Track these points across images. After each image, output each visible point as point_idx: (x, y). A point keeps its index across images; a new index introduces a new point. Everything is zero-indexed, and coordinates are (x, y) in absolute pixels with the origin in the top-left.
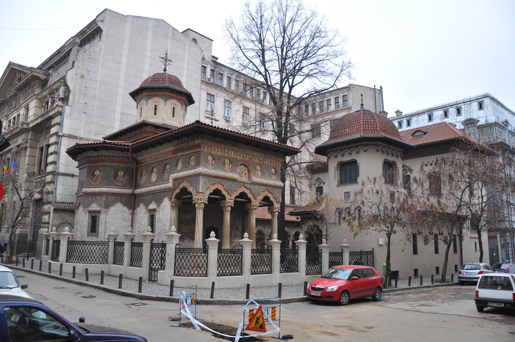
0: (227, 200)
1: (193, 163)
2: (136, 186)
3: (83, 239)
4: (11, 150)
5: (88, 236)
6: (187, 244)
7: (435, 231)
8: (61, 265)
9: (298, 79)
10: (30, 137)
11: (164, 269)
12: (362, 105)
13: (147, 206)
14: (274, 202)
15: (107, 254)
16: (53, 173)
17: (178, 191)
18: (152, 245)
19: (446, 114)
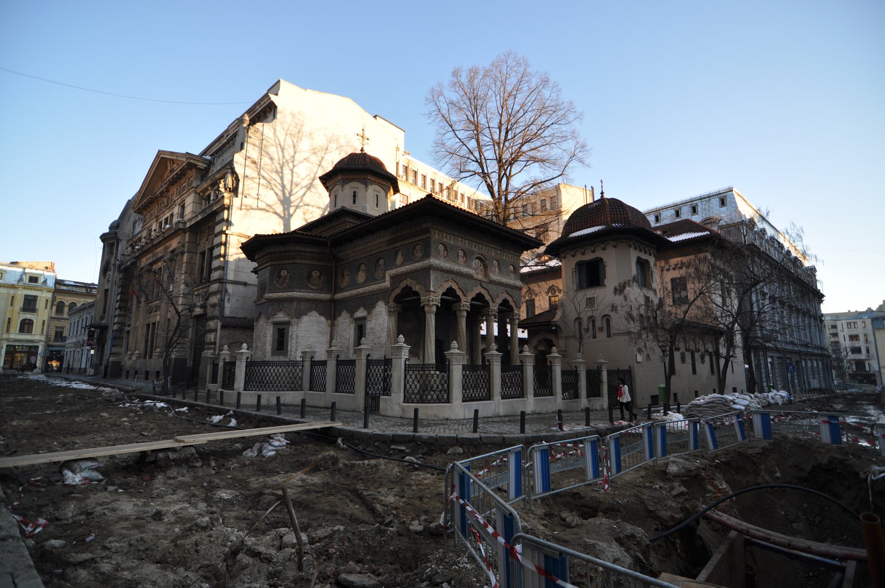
2: (338, 289)
3: (266, 359)
5: (274, 353)
8: (239, 394)
10: (187, 240)
11: (387, 395)
12: (602, 193)
14: (514, 308)
15: (301, 378)
17: (398, 291)
18: (369, 363)
19: (678, 214)
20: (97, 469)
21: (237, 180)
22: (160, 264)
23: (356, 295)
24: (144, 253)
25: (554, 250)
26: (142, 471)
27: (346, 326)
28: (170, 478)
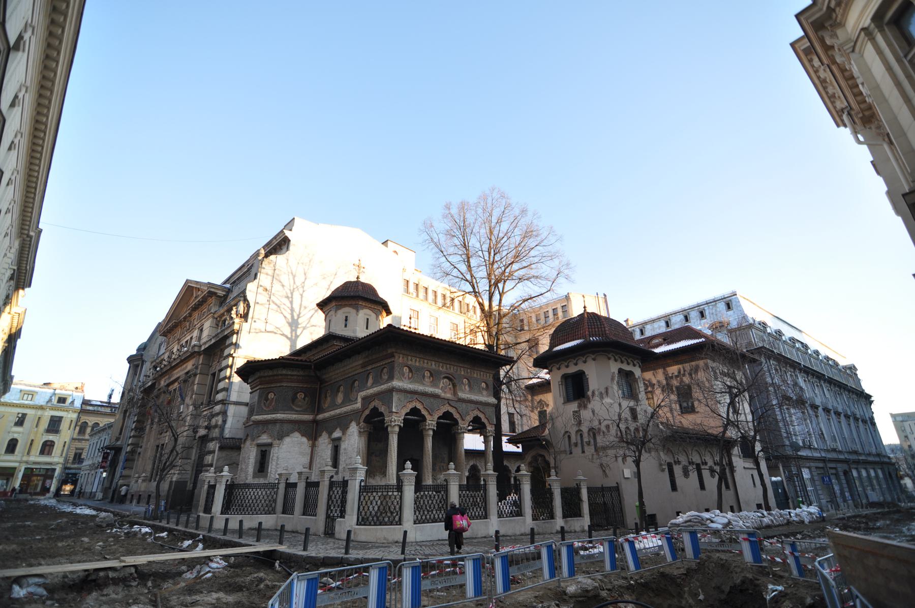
0: (428, 422)
1: (385, 377)
2: (320, 410)
3: (247, 482)
4: (178, 378)
5: (254, 477)
6: (377, 481)
7: (696, 459)
8: (212, 518)
9: (509, 284)
13: (330, 434)
14: (487, 425)
15: (275, 501)
16: (223, 402)
17: (367, 412)
18: (332, 484)
19: (687, 319)
20: (45, 586)
21: (248, 306)
22: (176, 384)
23: (334, 416)
24: (163, 374)
25: (541, 362)
26: (82, 588)
27: (324, 445)
28: (103, 595)
